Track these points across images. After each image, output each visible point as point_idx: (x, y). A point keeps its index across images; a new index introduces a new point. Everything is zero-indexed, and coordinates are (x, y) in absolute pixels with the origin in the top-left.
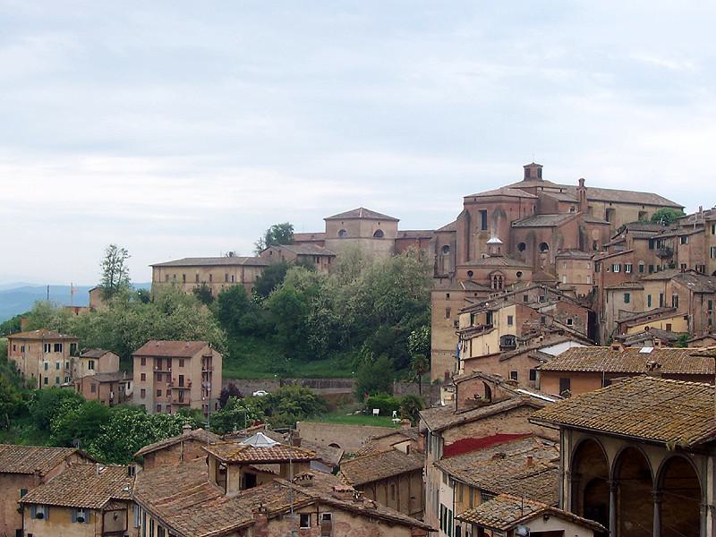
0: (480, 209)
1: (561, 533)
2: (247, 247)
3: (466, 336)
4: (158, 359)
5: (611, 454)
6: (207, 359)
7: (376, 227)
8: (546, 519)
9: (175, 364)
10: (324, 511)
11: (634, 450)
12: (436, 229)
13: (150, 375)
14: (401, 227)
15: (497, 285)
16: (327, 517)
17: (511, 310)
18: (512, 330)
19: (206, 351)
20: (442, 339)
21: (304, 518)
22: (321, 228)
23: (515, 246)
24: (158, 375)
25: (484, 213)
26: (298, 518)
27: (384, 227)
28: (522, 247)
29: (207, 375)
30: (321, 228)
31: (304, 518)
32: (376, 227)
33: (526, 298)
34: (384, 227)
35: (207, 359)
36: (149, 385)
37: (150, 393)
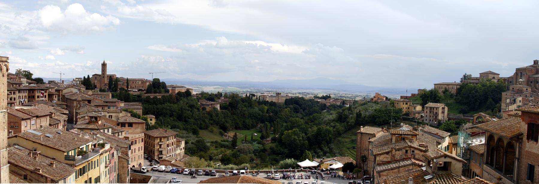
2: (458, 81)
3: (508, 105)
4: (431, 108)
5: (496, 138)
6: (443, 108)
8: (445, 158)
9: (435, 109)
10: (412, 149)
11: (500, 139)
12: (508, 77)
13: (428, 112)
15: (520, 92)
16: (413, 151)
17: (520, 99)
18: (521, 104)
19: (443, 106)
20: (503, 106)
21: (407, 151)
22: (478, 76)
23: (529, 82)
24: (430, 112)
26: (405, 151)
27: (495, 76)
29: (443, 112)
30: (478, 76)
31: (407, 151)
35: (443, 108)
36: (428, 114)
37: (428, 116)
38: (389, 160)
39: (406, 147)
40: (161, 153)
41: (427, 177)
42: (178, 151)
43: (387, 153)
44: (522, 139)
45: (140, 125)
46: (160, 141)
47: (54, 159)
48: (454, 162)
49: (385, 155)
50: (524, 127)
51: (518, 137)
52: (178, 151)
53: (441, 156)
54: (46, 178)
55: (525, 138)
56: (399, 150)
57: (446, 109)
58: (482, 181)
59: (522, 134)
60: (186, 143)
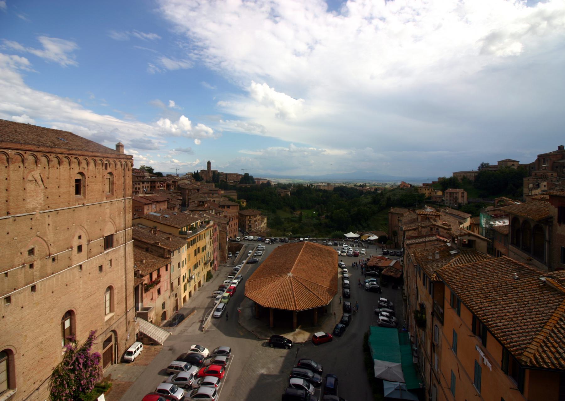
0: (542, 158)
1: (475, 241)
2: (476, 169)
4: (451, 193)
5: (521, 221)
6: (463, 193)
7: (512, 163)
10: (436, 227)
11: (526, 222)
13: (448, 196)
14: (520, 163)
15: (544, 177)
16: (437, 229)
21: (431, 229)
22: (497, 164)
23: (554, 167)
24: (450, 196)
25: (544, 159)
26: (429, 228)
28: (557, 167)
29: (463, 197)
30: (497, 164)
31: (431, 229)
32: (512, 163)
33: (552, 181)
34: (515, 163)
35: (463, 193)
36: (448, 198)
38: (416, 235)
39: (430, 225)
40: (250, 226)
41: (453, 252)
42: (262, 225)
43: (415, 230)
44: (552, 222)
45: (235, 207)
46: (250, 218)
47: (170, 234)
48: (478, 241)
49: (413, 231)
50: (554, 211)
51: (548, 220)
52: (262, 225)
53: (465, 235)
54: (164, 249)
55: (555, 222)
56: (424, 227)
57: (466, 194)
58: (510, 260)
59: (552, 218)
60: (268, 219)
